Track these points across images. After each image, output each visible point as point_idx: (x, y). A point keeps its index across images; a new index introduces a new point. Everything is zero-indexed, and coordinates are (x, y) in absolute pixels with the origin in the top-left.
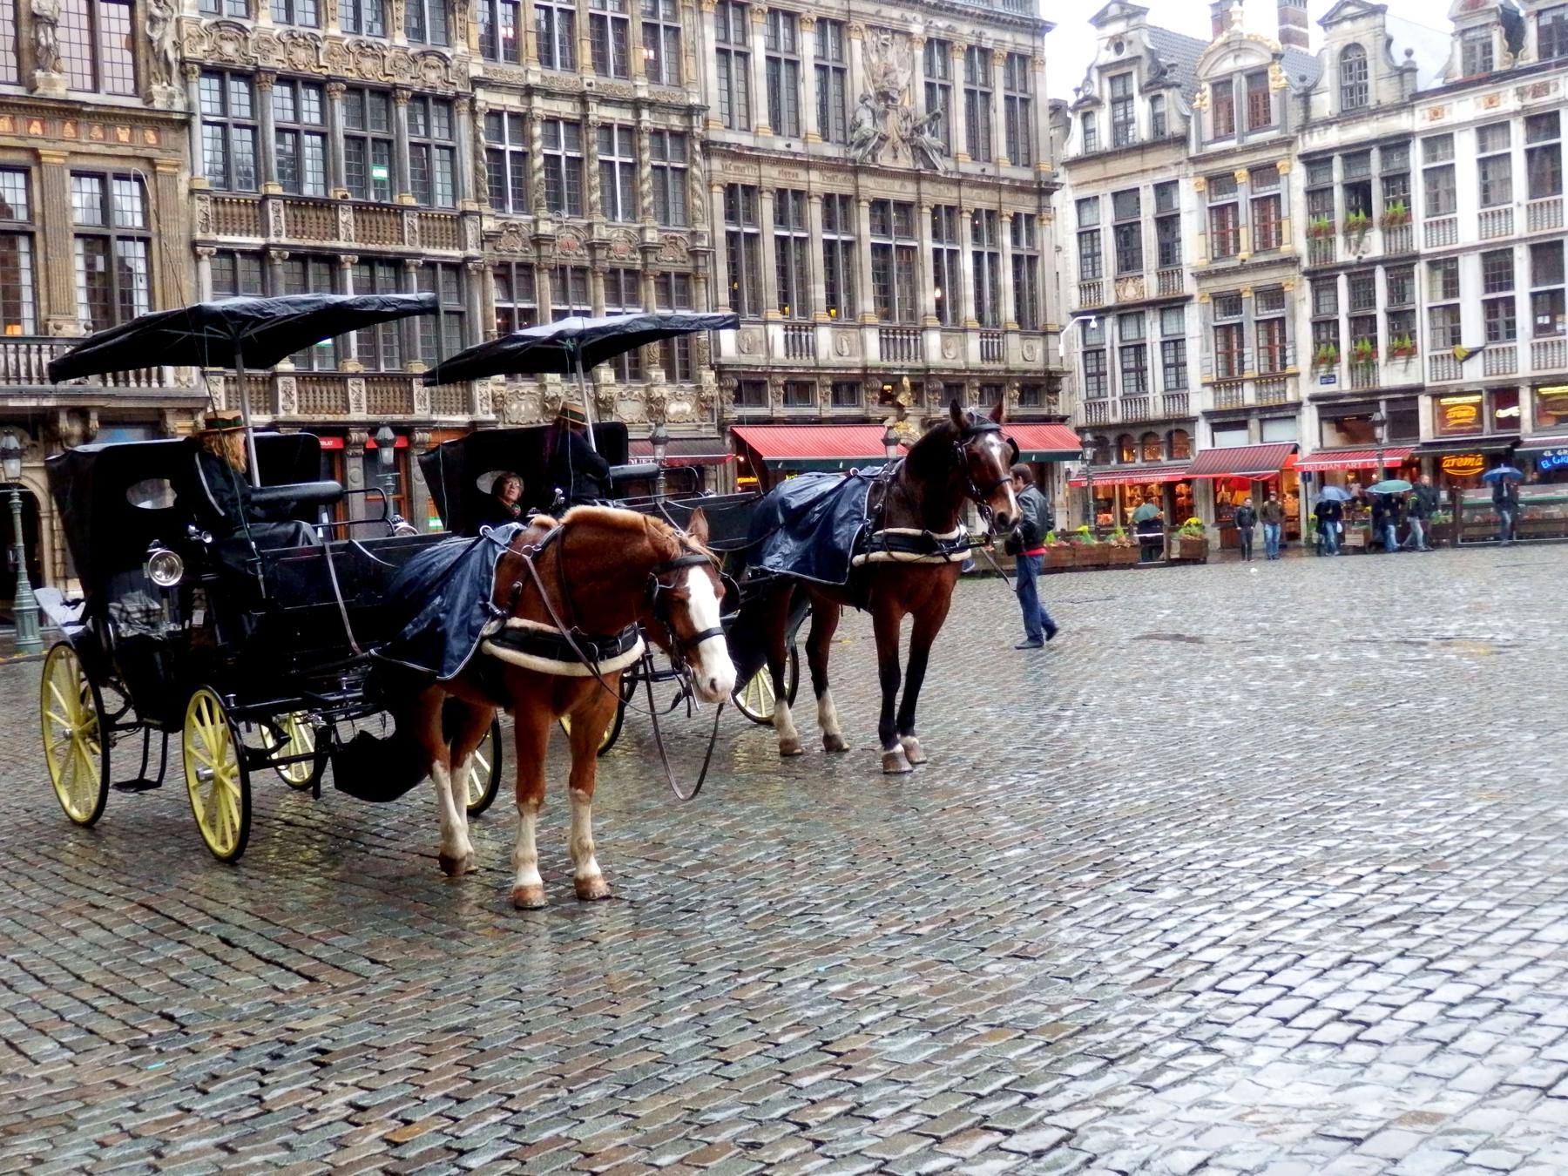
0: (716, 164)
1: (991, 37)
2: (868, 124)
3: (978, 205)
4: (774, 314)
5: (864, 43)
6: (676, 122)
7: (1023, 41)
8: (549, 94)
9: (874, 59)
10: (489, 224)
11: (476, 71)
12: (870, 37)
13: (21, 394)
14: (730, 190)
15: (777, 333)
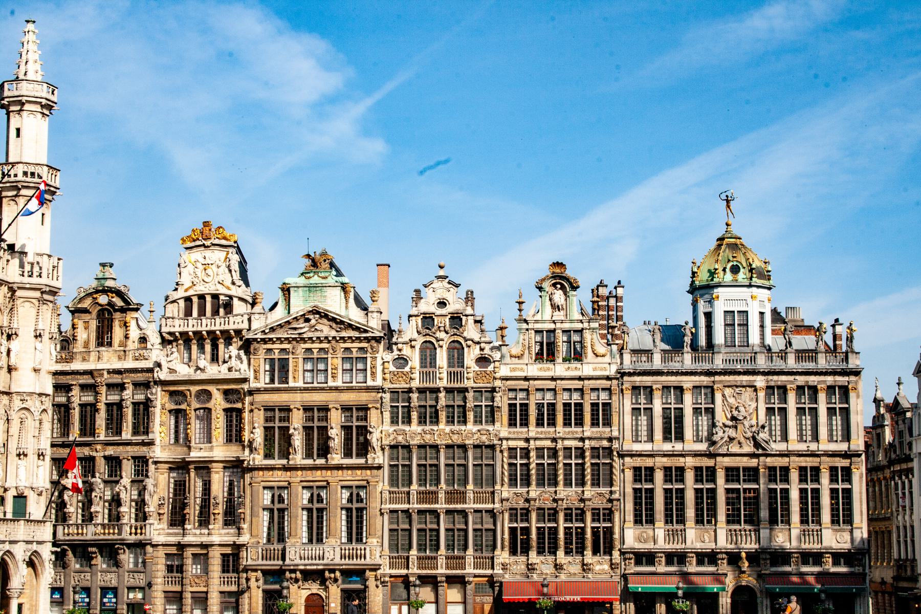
0: (627, 459)
1: (813, 380)
2: (720, 434)
3: (803, 464)
4: (660, 523)
5: (724, 396)
6: (605, 443)
7: (841, 380)
8: (535, 439)
9: (731, 400)
10: (505, 495)
11: (504, 434)
12: (728, 391)
13: (310, 565)
14: (637, 470)
15: (660, 533)
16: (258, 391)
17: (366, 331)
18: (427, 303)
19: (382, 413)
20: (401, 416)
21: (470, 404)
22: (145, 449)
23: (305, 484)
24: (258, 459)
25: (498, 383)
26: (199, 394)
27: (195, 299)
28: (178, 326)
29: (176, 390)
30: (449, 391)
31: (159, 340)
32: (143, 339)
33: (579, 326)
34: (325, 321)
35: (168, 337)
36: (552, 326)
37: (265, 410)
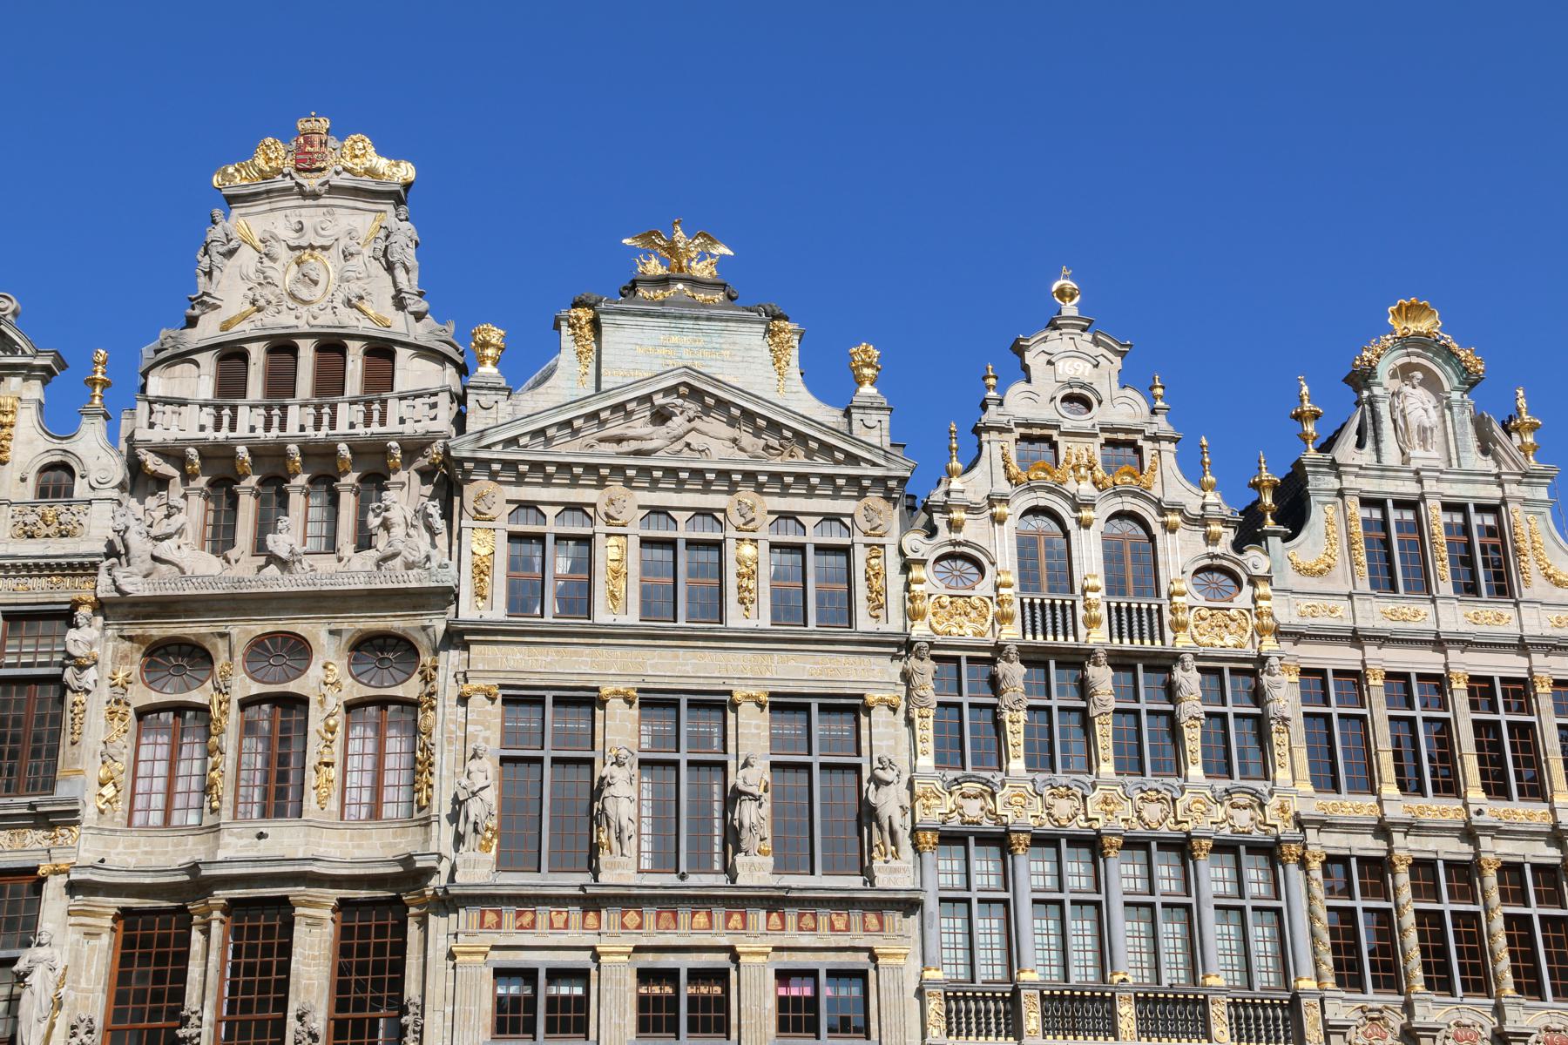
8: (1412, 828)
16: (488, 633)
17: (853, 459)
18: (1032, 397)
19: (910, 722)
20: (968, 739)
21: (1192, 706)
22: (35, 839)
23: (649, 960)
24: (478, 868)
25: (1269, 645)
26: (259, 646)
27: (257, 352)
28: (191, 426)
29: (171, 639)
30: (1121, 662)
31: (118, 472)
32: (57, 479)
33: (1492, 493)
34: (716, 426)
35: (153, 463)
36: (1409, 489)
37: (506, 701)
